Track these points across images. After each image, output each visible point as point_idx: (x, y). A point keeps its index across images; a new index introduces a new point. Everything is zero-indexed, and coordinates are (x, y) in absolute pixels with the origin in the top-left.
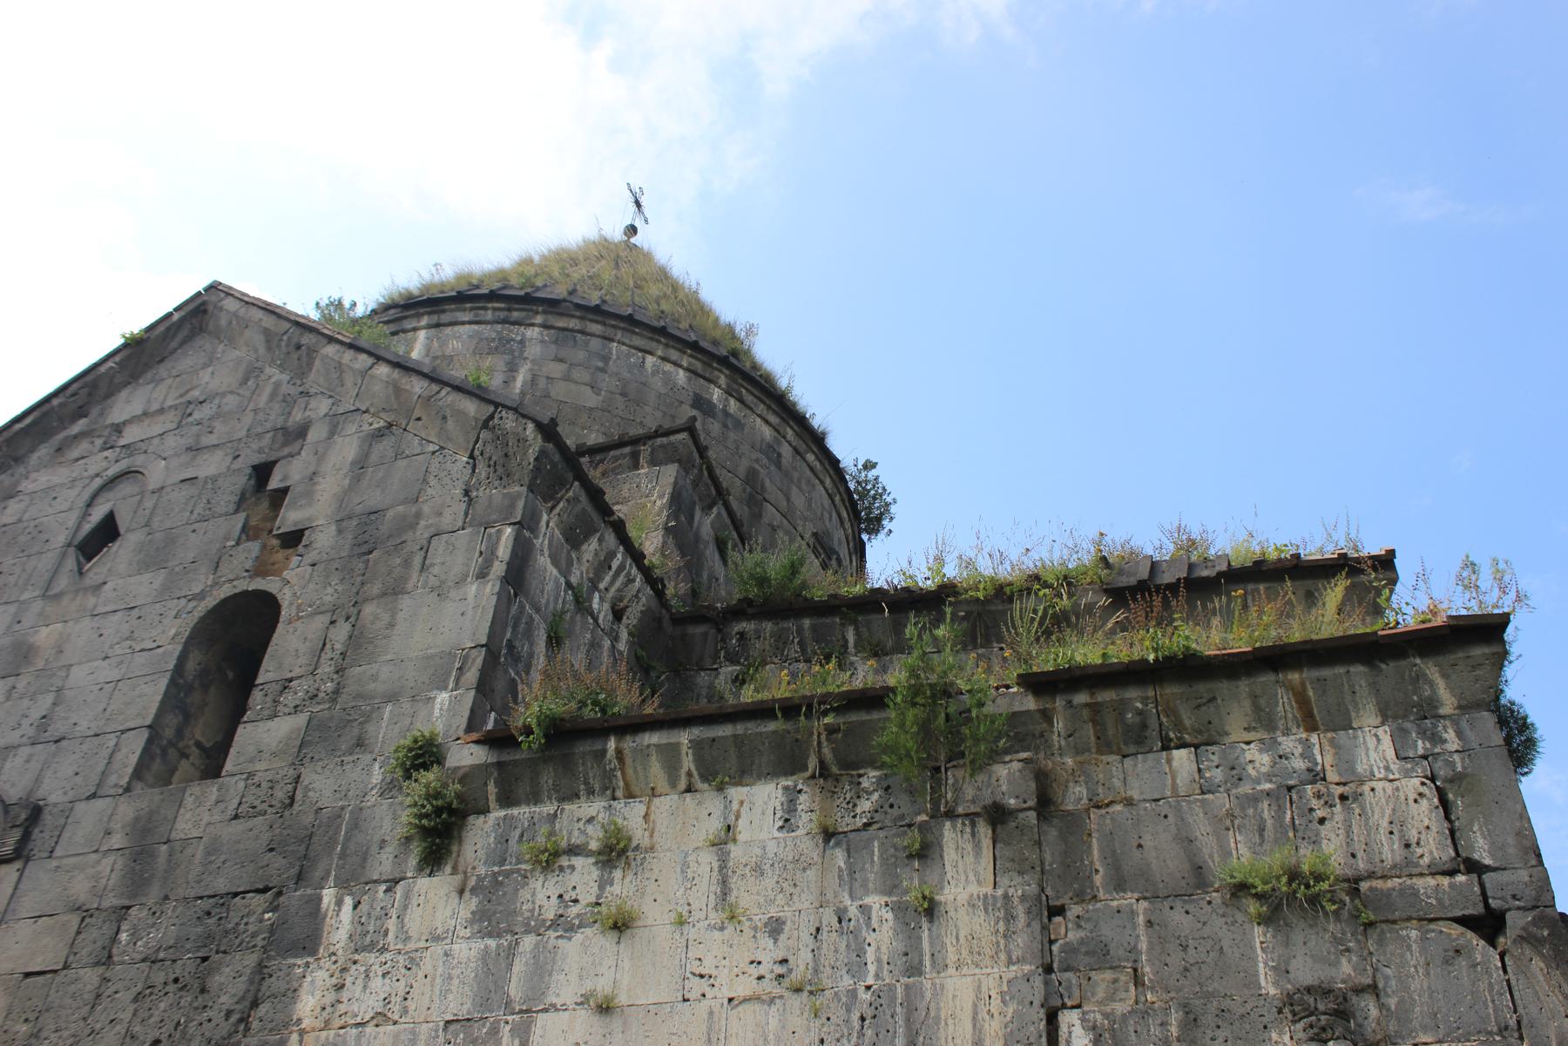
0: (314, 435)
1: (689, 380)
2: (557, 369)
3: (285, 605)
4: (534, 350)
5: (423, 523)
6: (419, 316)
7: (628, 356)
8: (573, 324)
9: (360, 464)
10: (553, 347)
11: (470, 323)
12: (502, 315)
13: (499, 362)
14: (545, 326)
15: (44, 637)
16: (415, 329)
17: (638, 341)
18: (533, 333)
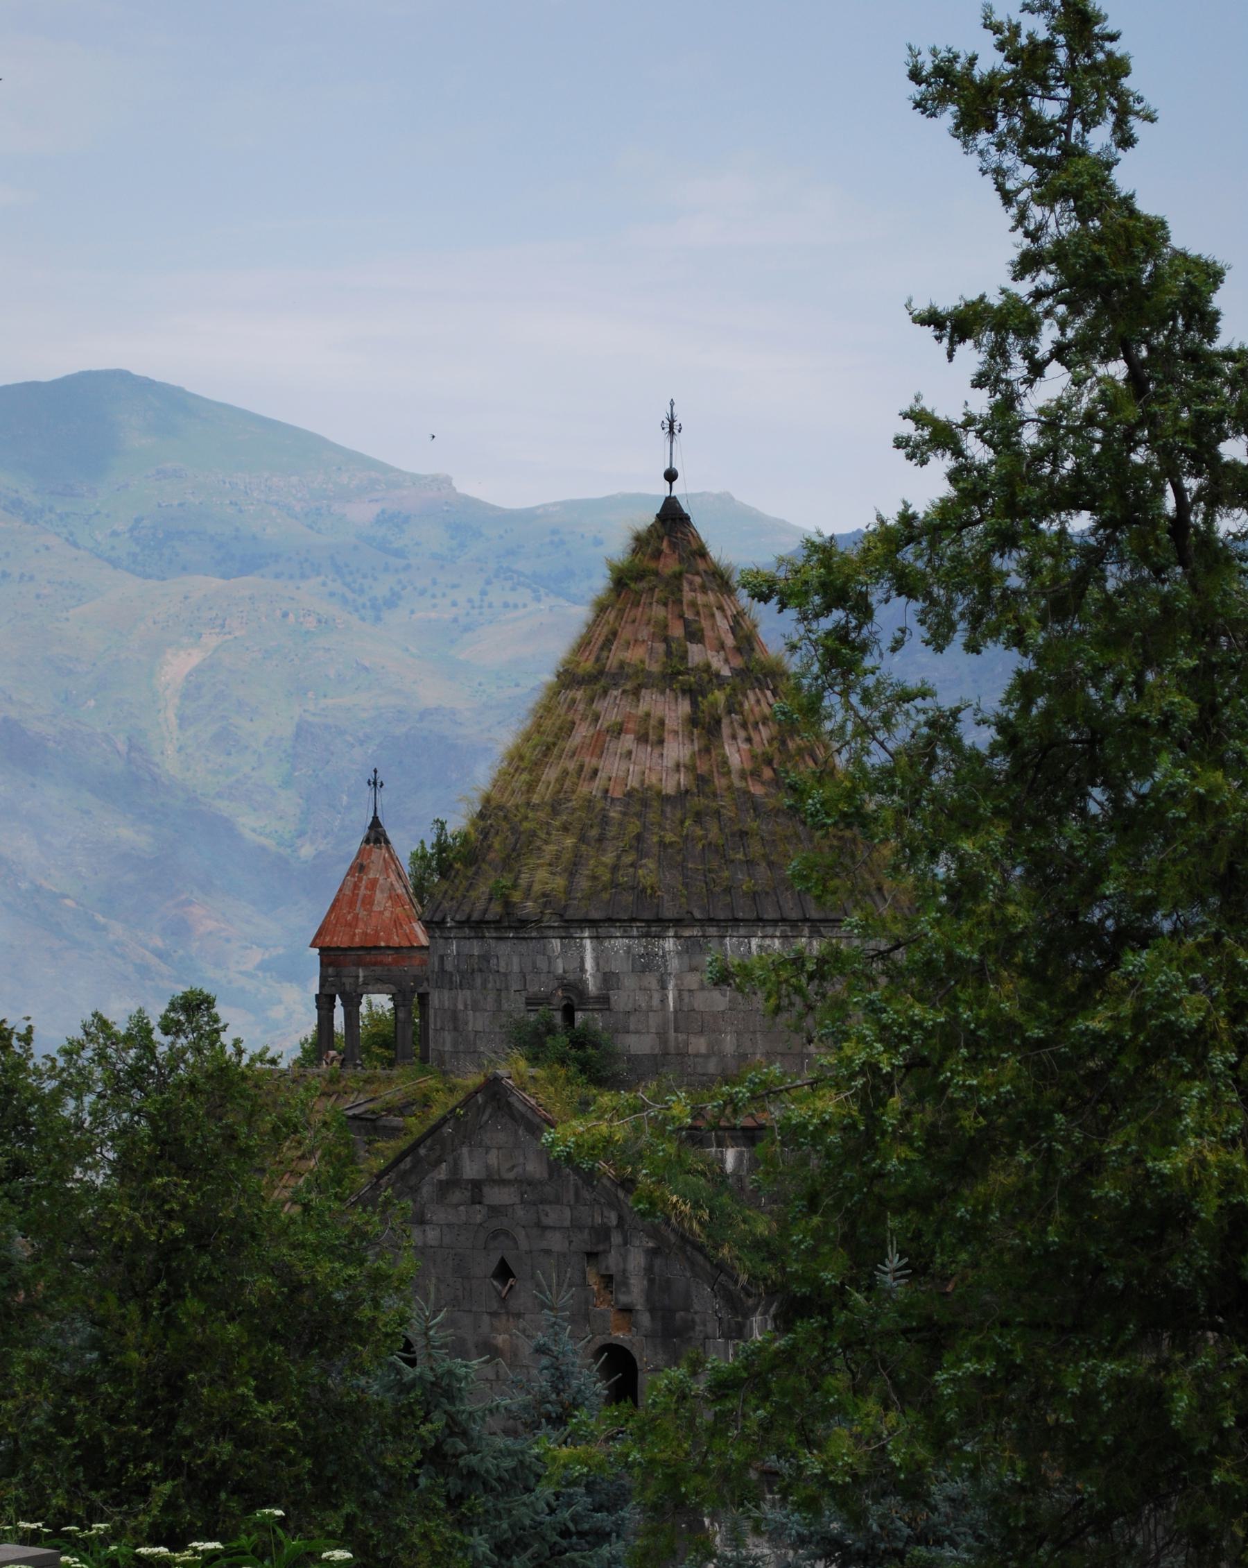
0: (616, 1238)
1: (782, 944)
2: (692, 980)
3: (636, 1353)
4: (674, 964)
5: (697, 1328)
6: (582, 929)
7: (740, 944)
8: (695, 932)
9: (649, 1269)
10: (686, 957)
11: (622, 937)
12: (645, 930)
13: (651, 981)
14: (676, 936)
15: (500, 1339)
16: (582, 938)
17: (742, 931)
18: (669, 944)
